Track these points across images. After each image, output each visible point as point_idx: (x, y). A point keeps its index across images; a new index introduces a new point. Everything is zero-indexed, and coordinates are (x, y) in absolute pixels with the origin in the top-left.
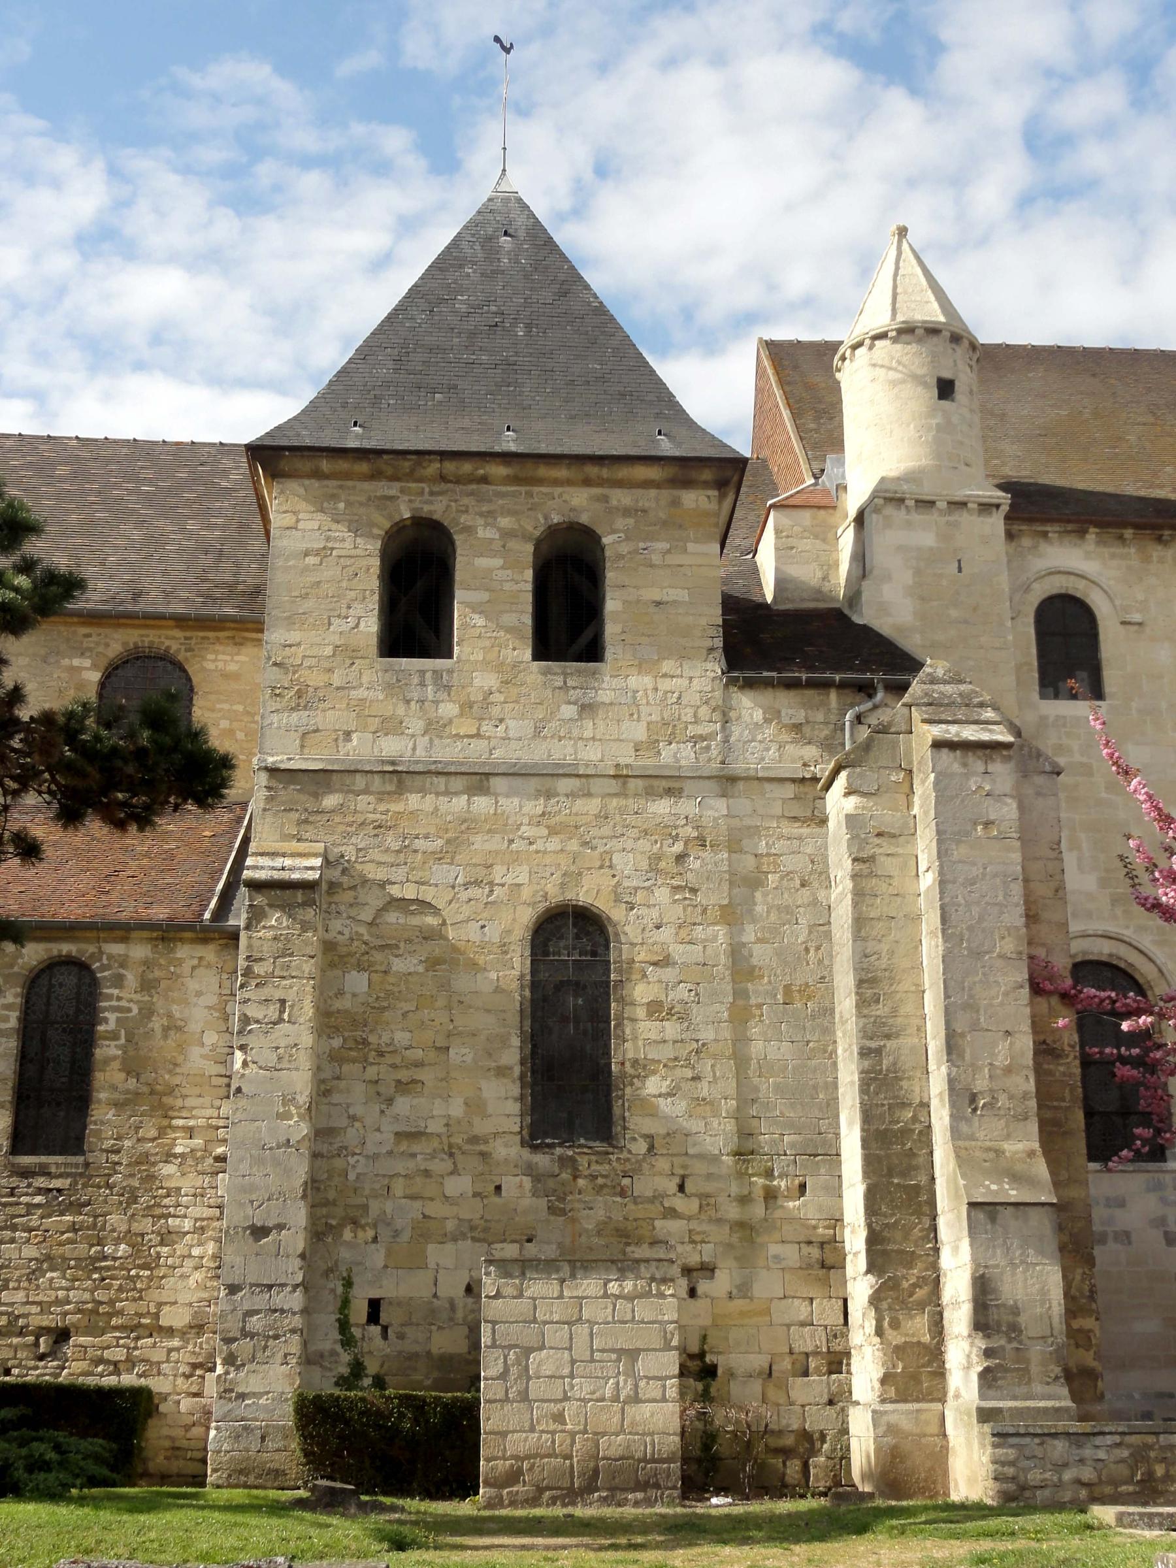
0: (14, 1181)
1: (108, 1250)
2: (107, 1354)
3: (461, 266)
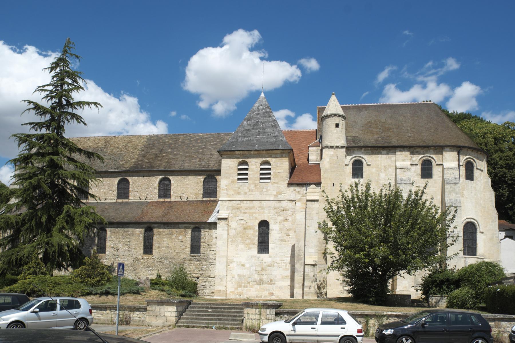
0: (191, 258)
1: (204, 267)
2: (204, 280)
3: (254, 113)
